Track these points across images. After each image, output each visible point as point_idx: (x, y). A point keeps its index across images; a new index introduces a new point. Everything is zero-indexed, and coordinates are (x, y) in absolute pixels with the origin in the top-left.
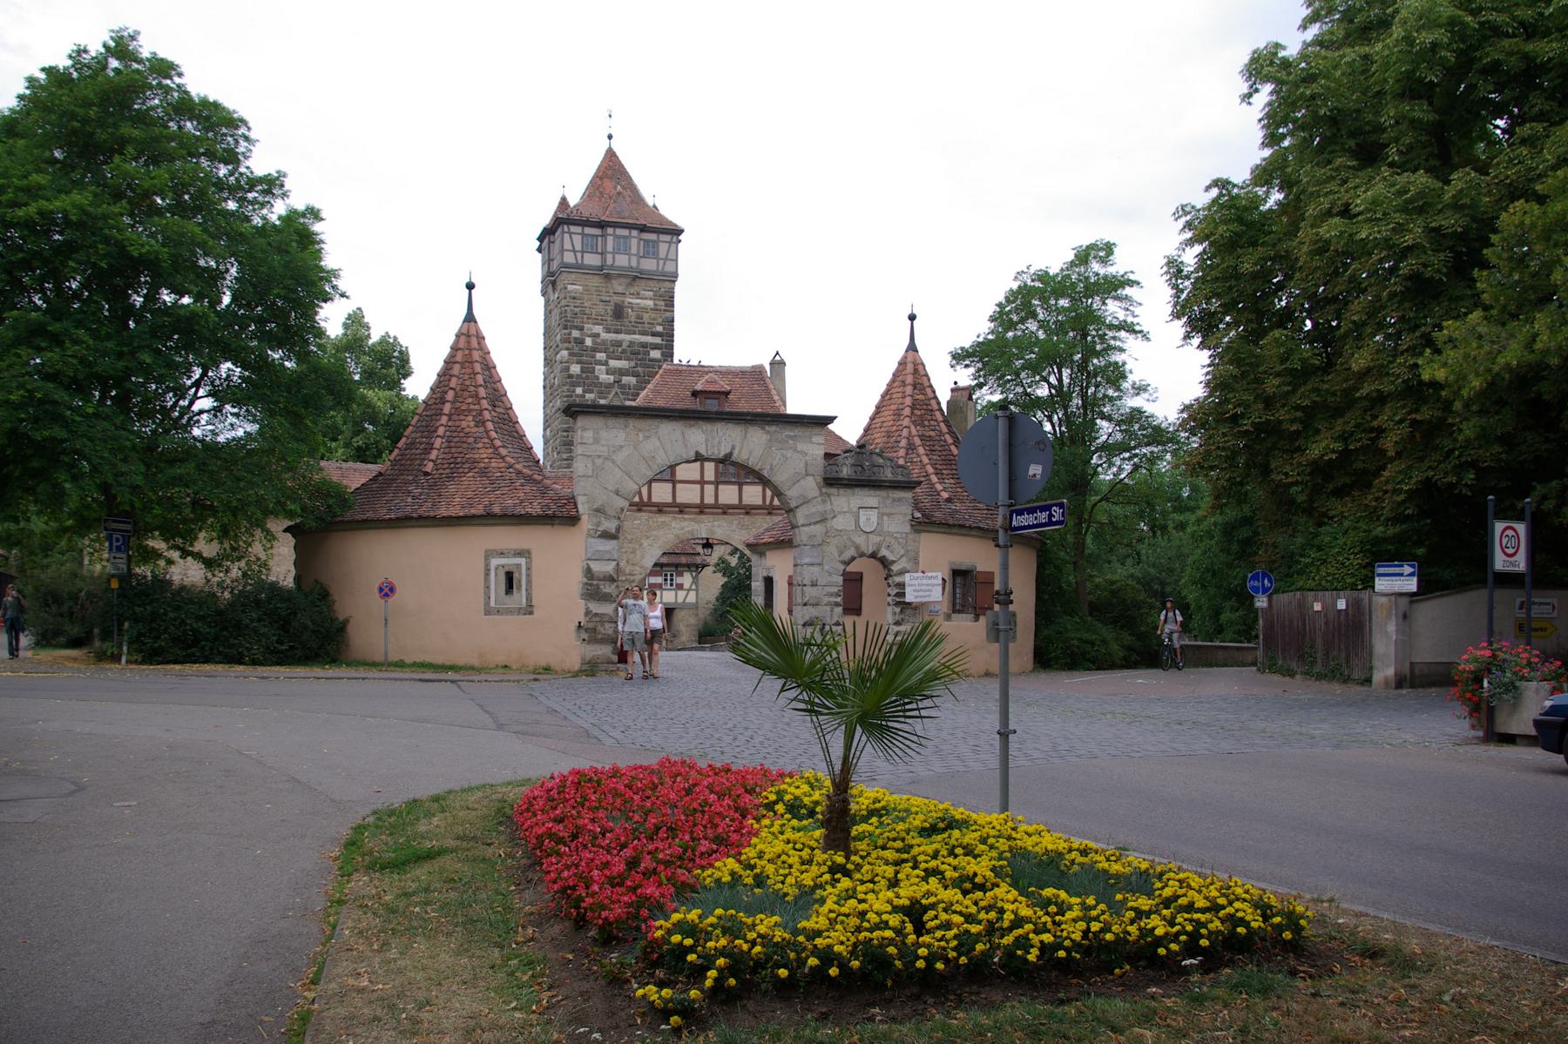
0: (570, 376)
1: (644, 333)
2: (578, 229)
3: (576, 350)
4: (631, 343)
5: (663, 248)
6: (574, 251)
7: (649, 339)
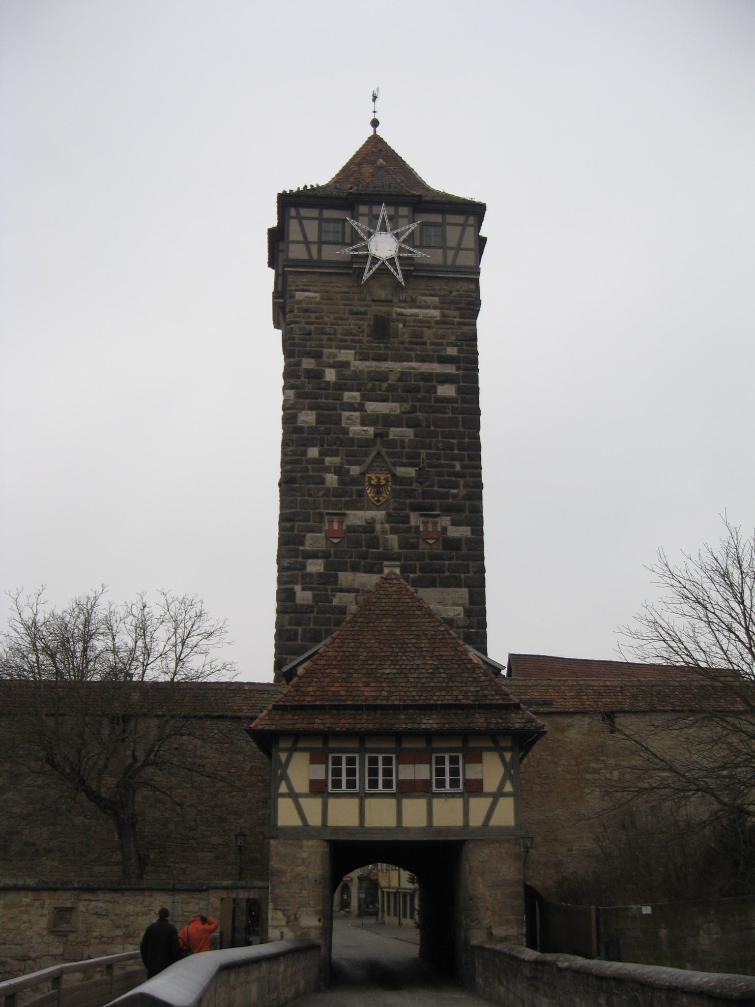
0: (300, 430)
1: (424, 359)
2: (314, 213)
3: (309, 388)
4: (404, 376)
5: (452, 235)
6: (307, 243)
7: (436, 368)
